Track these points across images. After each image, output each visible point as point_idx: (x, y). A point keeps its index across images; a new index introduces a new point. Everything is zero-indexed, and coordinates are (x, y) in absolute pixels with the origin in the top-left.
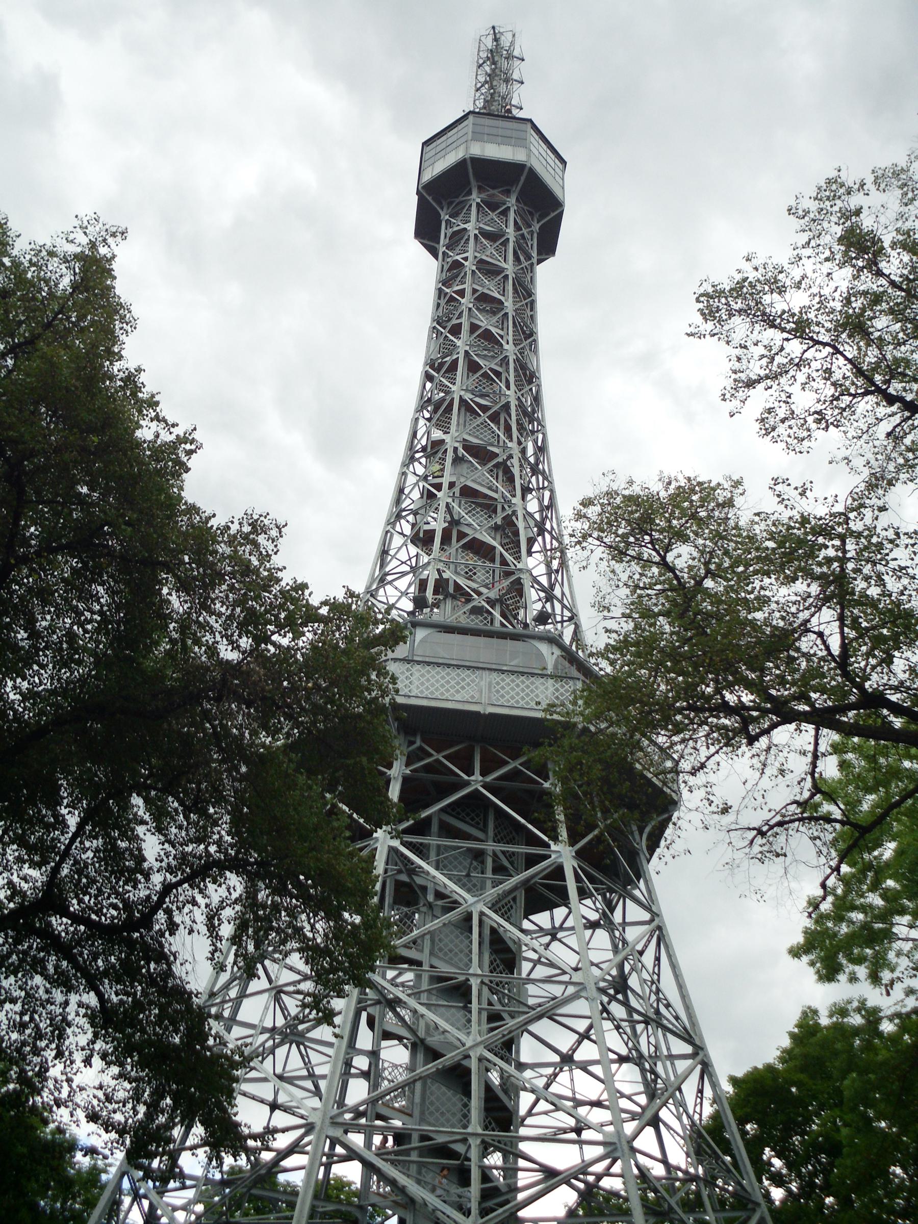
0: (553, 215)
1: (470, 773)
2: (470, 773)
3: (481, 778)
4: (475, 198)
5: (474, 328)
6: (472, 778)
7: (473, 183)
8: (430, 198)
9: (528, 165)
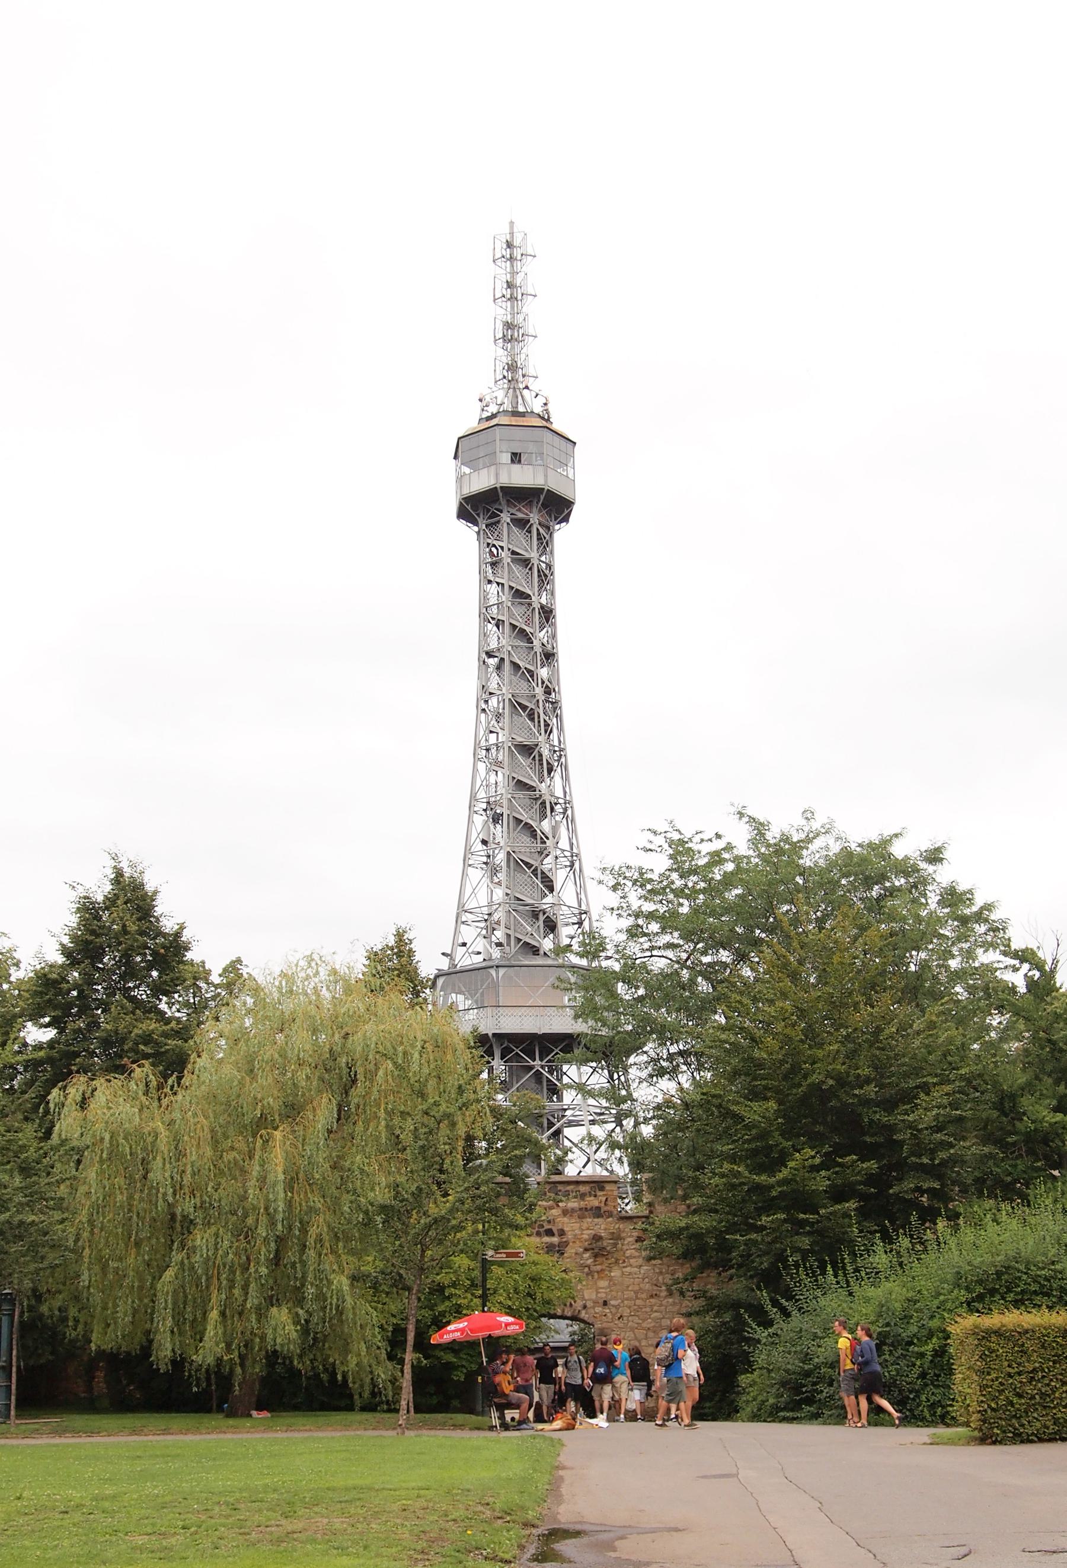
0: (566, 512)
1: (534, 1060)
2: (534, 1060)
3: (540, 1063)
4: (505, 517)
5: (516, 666)
6: (535, 1063)
7: (503, 502)
8: (469, 508)
9: (546, 488)
